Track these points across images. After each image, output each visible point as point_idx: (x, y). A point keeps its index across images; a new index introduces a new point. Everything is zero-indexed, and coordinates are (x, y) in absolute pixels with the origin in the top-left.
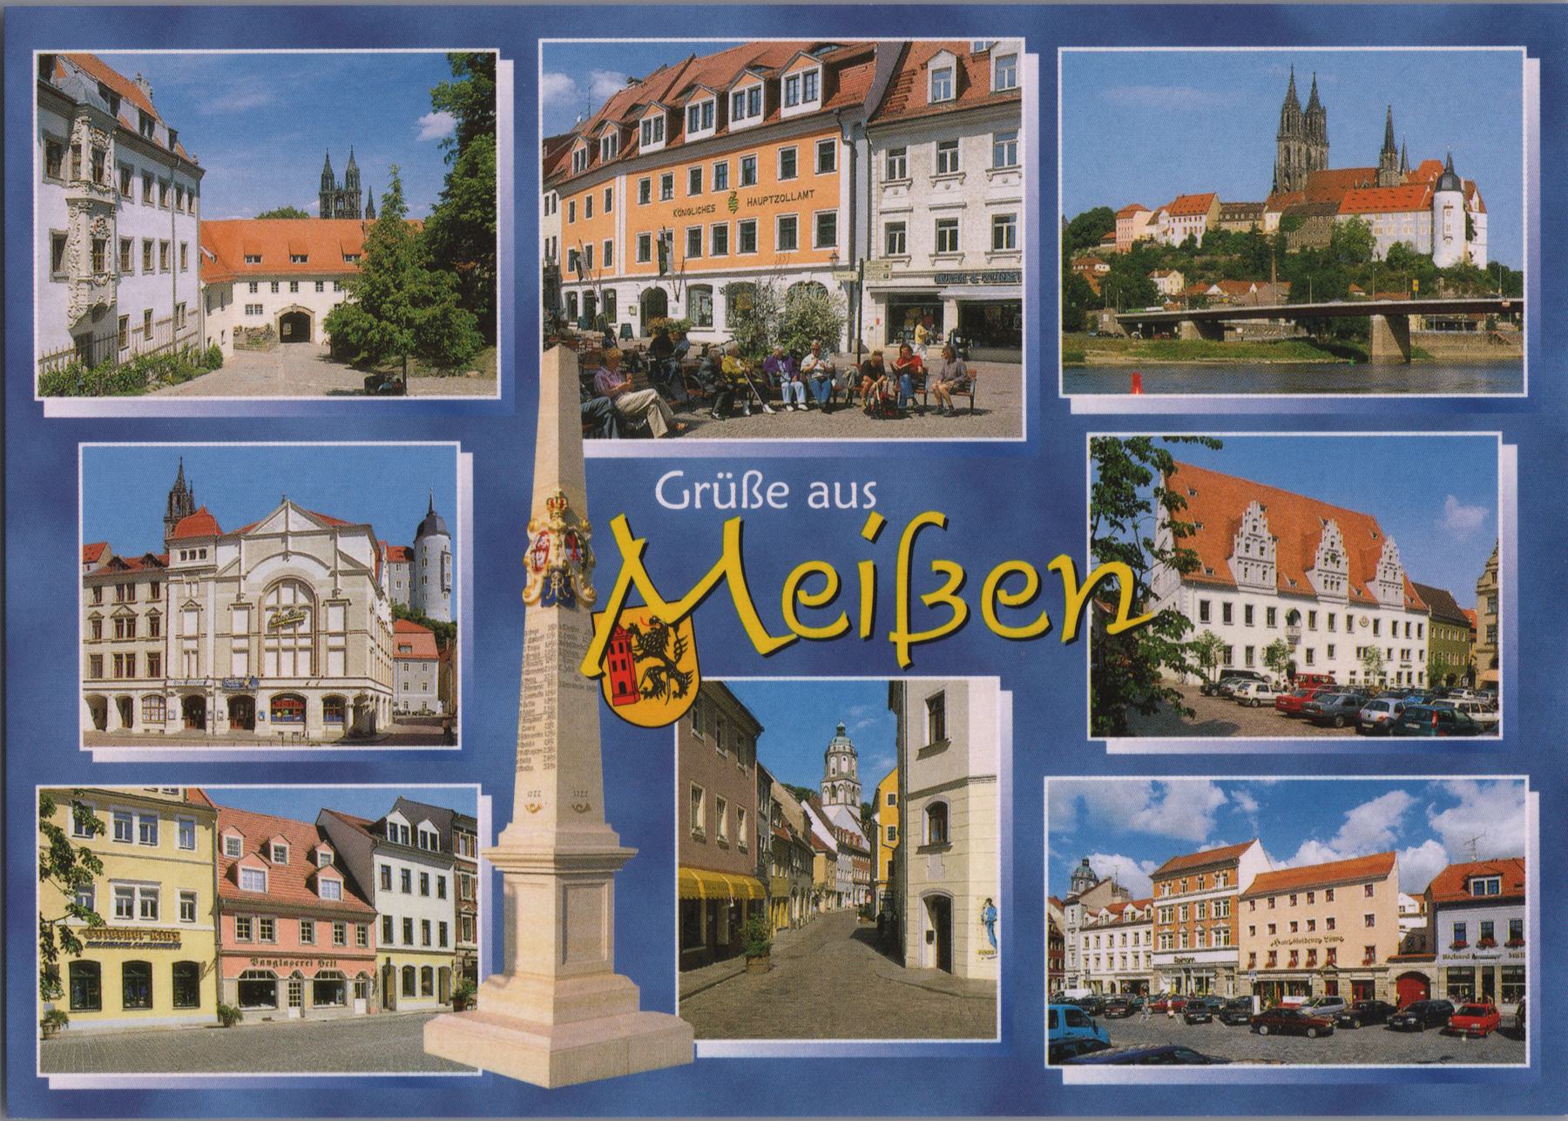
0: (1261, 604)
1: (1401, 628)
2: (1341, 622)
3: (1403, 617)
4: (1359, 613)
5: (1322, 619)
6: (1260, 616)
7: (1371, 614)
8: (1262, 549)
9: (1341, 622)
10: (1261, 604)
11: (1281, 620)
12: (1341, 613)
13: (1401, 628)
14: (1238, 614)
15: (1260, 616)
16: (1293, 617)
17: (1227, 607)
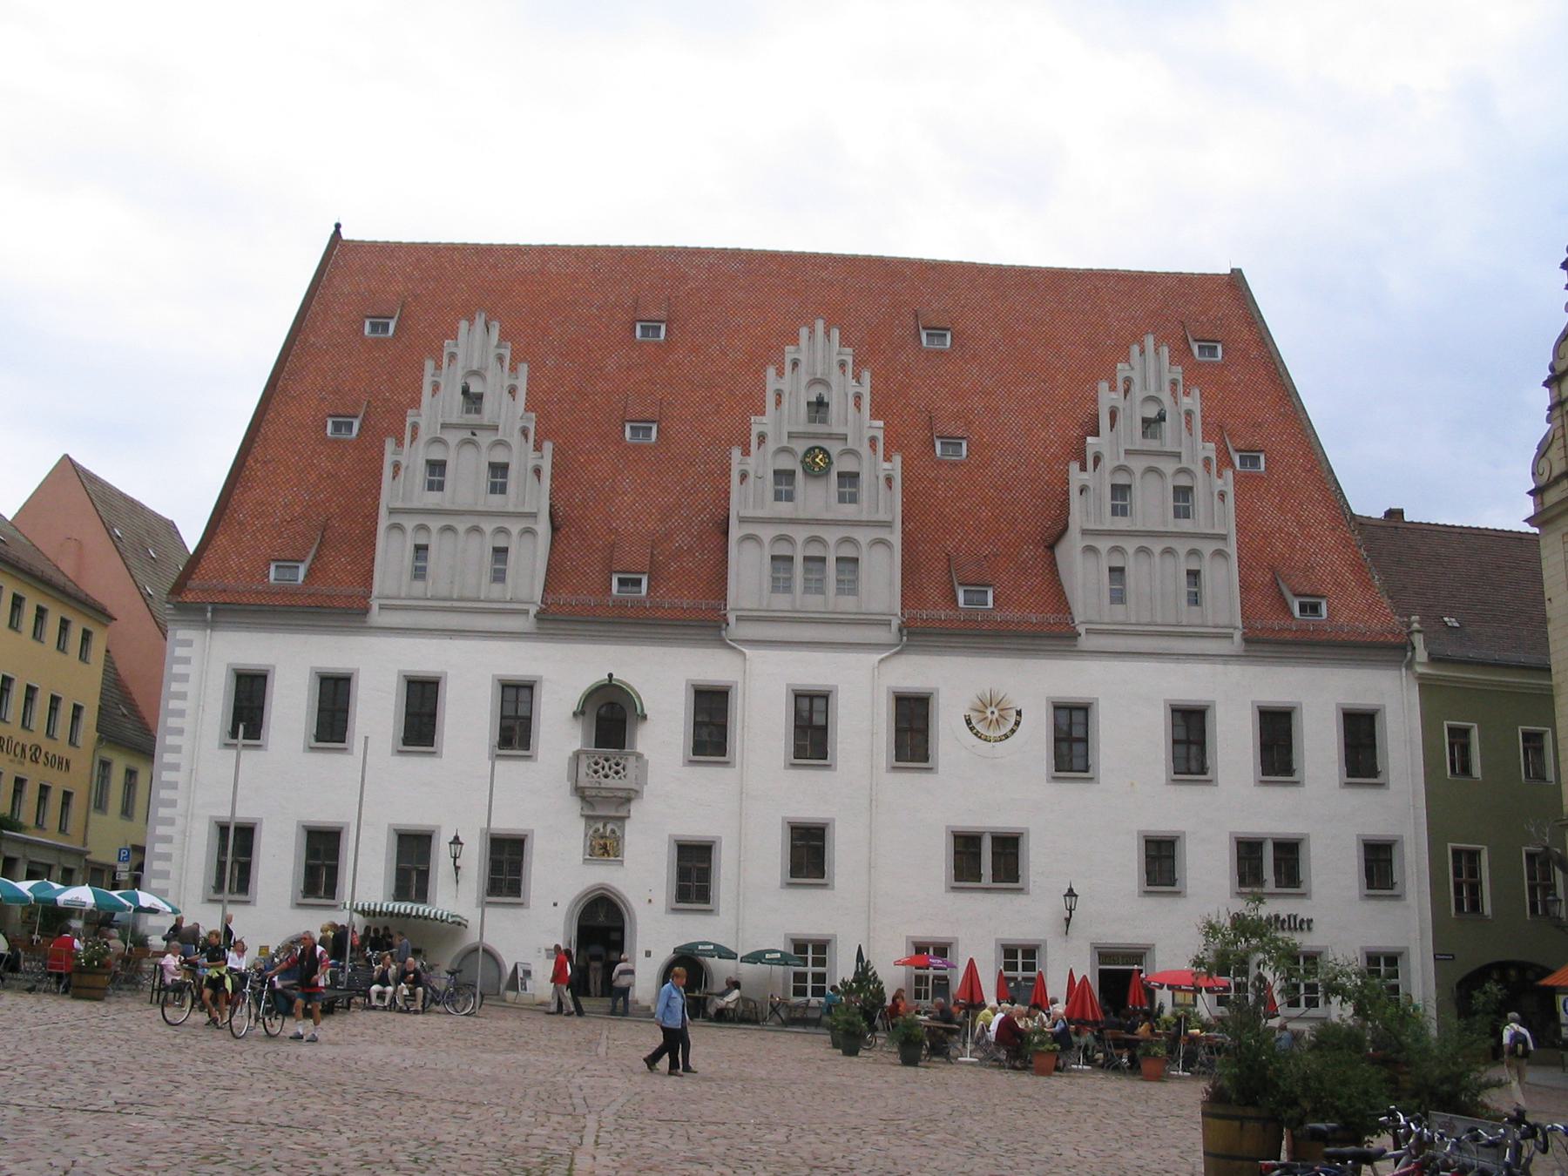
0: (470, 677)
1: (1234, 741)
2: (862, 727)
3: (1235, 694)
4: (955, 680)
5: (762, 724)
6: (468, 717)
7: (1034, 683)
8: (499, 469)
9: (862, 727)
10: (470, 677)
11: (559, 731)
12: (862, 690)
13: (1234, 741)
14: (376, 712)
15: (468, 717)
16: (611, 716)
17: (334, 695)
